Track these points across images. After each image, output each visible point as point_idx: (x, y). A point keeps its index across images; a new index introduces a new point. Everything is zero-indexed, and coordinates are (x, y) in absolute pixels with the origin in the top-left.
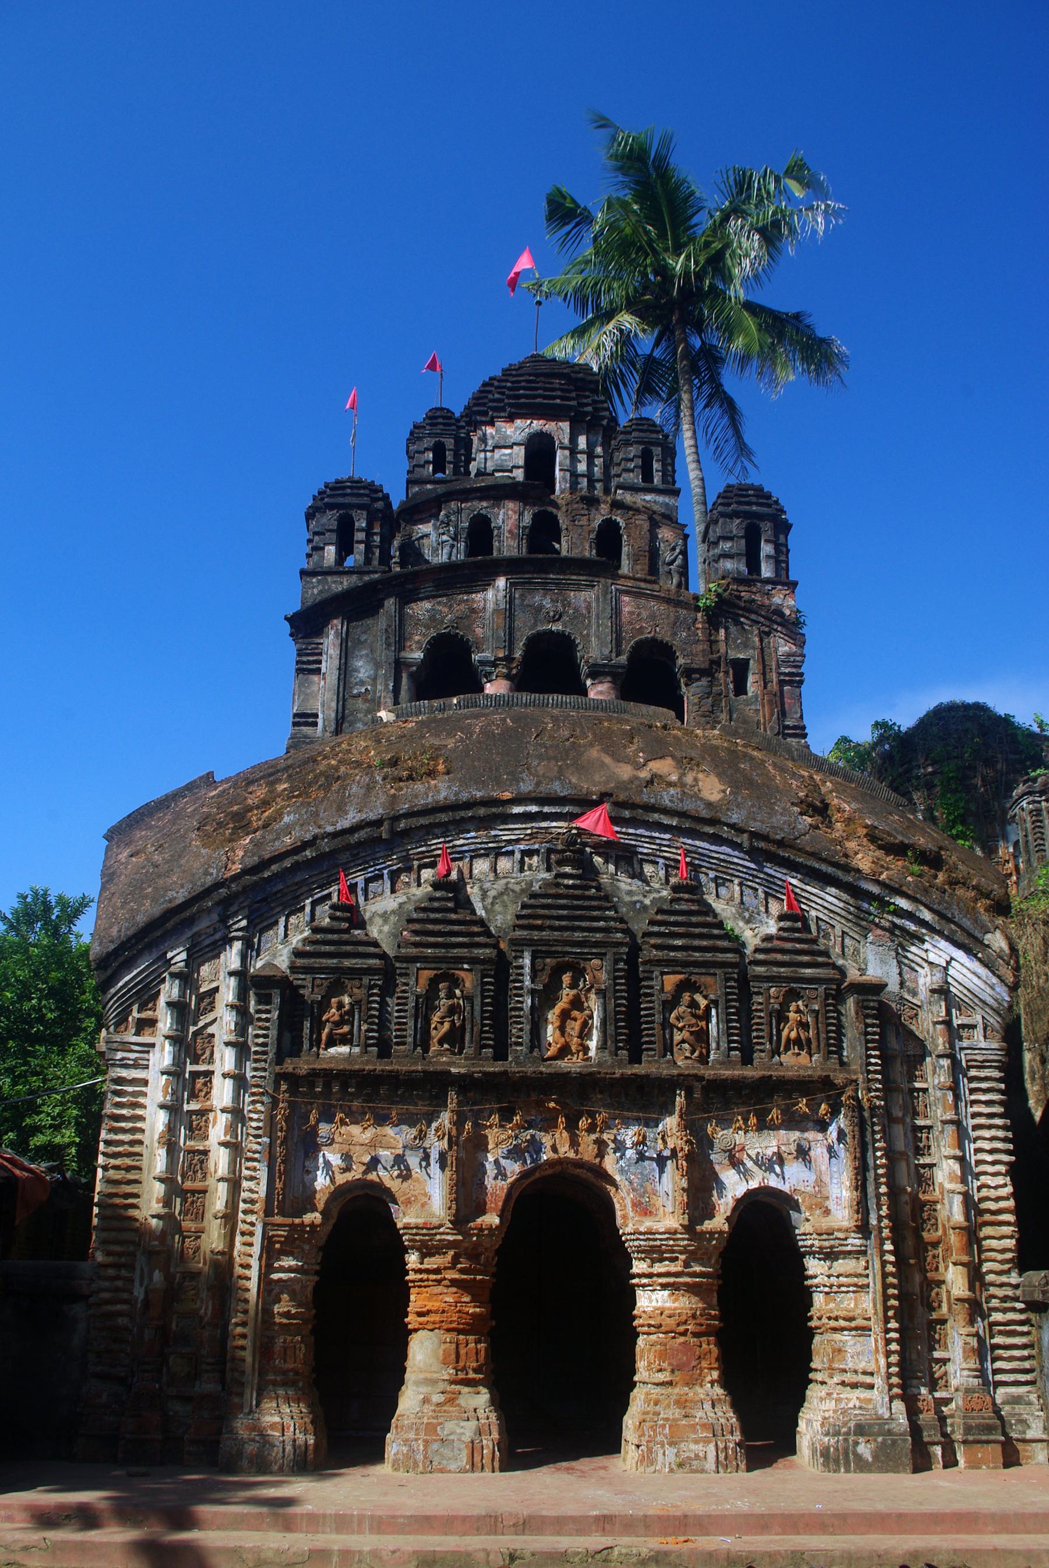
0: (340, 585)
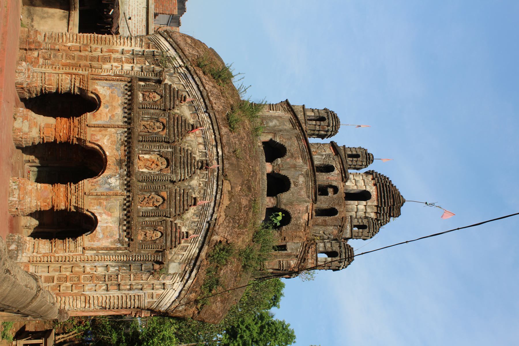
0: (300, 116)
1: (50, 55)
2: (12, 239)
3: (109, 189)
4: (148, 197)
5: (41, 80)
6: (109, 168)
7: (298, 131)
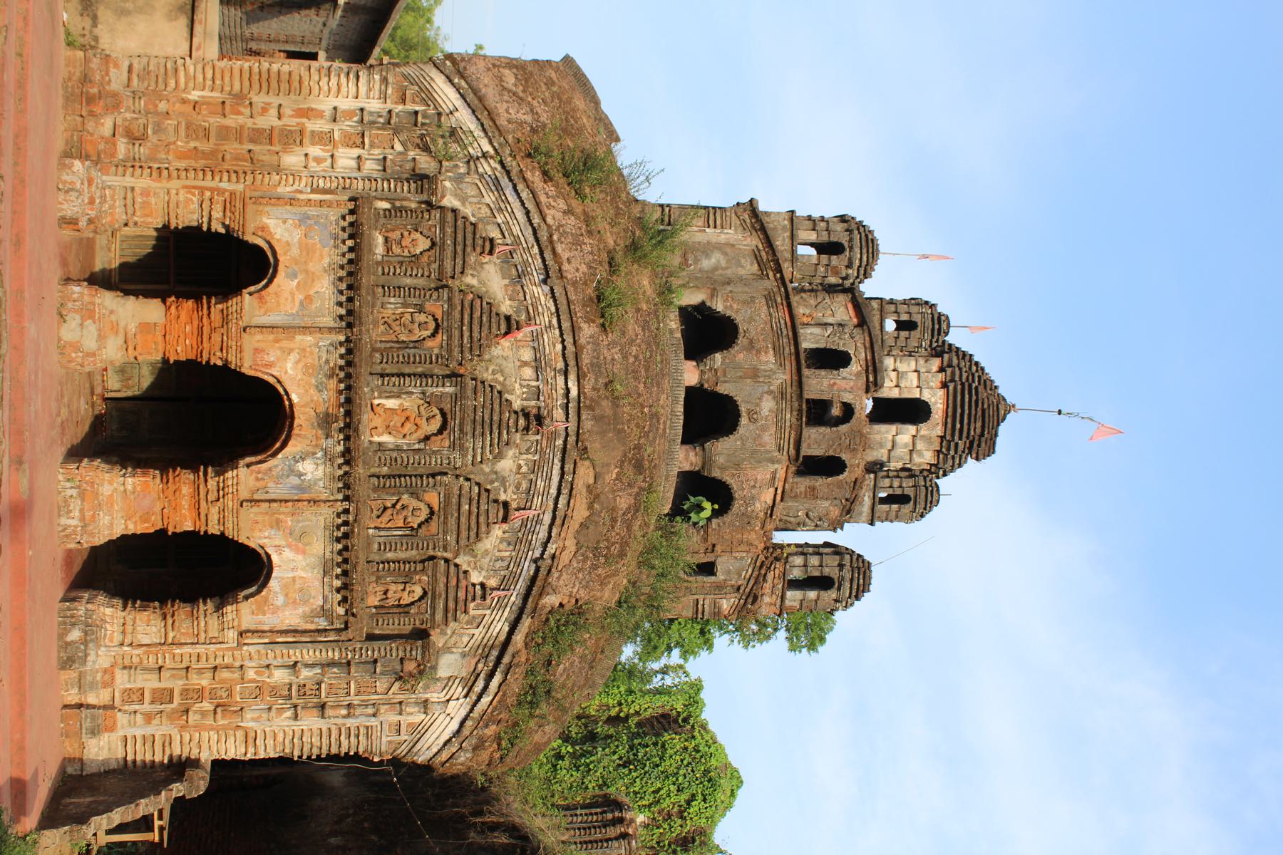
0: (781, 243)
1: (146, 127)
2: (72, 617)
3: (300, 488)
4: (394, 506)
5: (125, 206)
7: (771, 283)
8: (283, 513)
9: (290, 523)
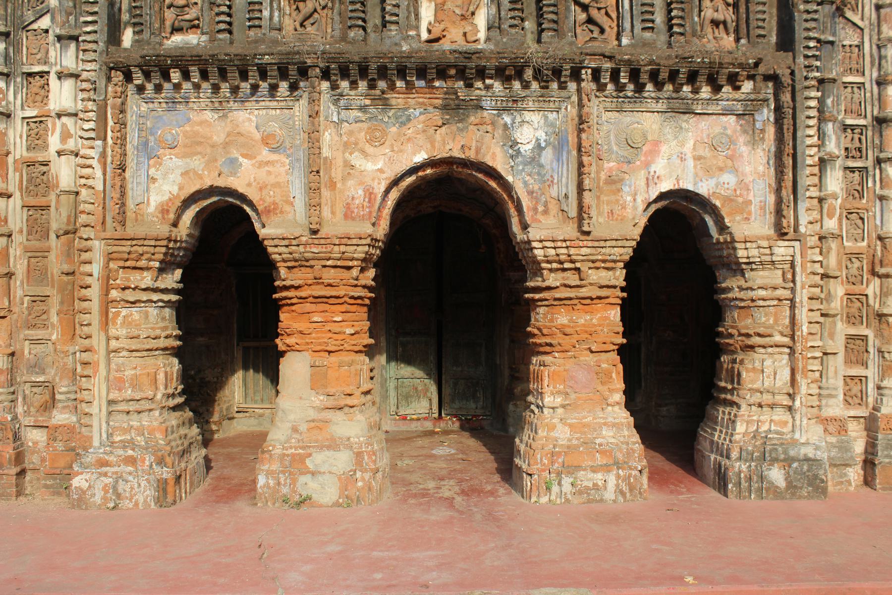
2: (750, 479)
3: (559, 148)
6: (478, 151)
8: (598, 172)
9: (612, 164)
